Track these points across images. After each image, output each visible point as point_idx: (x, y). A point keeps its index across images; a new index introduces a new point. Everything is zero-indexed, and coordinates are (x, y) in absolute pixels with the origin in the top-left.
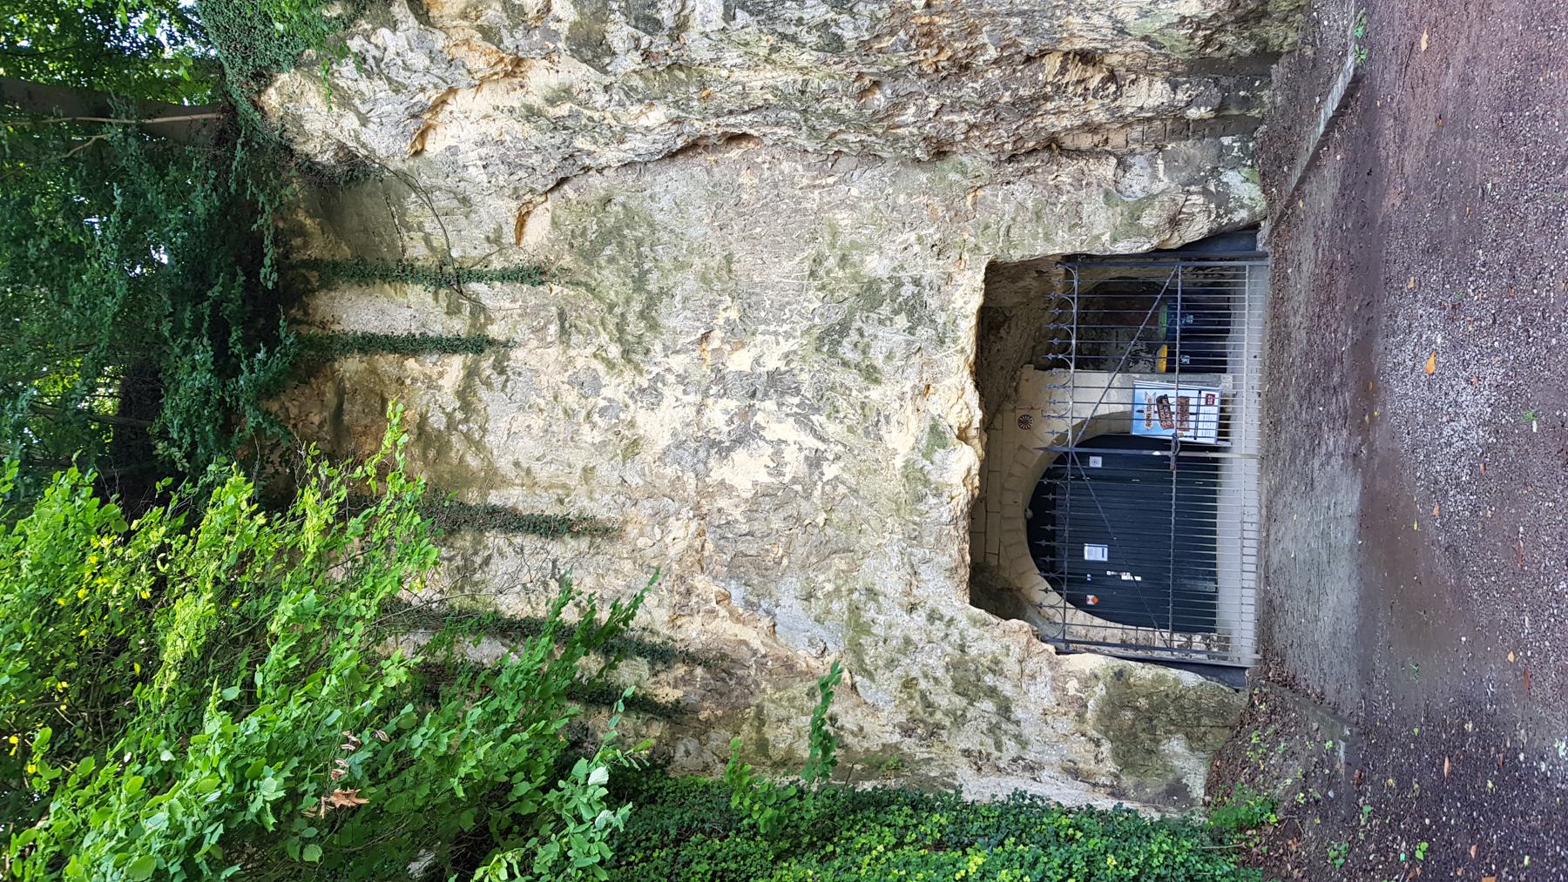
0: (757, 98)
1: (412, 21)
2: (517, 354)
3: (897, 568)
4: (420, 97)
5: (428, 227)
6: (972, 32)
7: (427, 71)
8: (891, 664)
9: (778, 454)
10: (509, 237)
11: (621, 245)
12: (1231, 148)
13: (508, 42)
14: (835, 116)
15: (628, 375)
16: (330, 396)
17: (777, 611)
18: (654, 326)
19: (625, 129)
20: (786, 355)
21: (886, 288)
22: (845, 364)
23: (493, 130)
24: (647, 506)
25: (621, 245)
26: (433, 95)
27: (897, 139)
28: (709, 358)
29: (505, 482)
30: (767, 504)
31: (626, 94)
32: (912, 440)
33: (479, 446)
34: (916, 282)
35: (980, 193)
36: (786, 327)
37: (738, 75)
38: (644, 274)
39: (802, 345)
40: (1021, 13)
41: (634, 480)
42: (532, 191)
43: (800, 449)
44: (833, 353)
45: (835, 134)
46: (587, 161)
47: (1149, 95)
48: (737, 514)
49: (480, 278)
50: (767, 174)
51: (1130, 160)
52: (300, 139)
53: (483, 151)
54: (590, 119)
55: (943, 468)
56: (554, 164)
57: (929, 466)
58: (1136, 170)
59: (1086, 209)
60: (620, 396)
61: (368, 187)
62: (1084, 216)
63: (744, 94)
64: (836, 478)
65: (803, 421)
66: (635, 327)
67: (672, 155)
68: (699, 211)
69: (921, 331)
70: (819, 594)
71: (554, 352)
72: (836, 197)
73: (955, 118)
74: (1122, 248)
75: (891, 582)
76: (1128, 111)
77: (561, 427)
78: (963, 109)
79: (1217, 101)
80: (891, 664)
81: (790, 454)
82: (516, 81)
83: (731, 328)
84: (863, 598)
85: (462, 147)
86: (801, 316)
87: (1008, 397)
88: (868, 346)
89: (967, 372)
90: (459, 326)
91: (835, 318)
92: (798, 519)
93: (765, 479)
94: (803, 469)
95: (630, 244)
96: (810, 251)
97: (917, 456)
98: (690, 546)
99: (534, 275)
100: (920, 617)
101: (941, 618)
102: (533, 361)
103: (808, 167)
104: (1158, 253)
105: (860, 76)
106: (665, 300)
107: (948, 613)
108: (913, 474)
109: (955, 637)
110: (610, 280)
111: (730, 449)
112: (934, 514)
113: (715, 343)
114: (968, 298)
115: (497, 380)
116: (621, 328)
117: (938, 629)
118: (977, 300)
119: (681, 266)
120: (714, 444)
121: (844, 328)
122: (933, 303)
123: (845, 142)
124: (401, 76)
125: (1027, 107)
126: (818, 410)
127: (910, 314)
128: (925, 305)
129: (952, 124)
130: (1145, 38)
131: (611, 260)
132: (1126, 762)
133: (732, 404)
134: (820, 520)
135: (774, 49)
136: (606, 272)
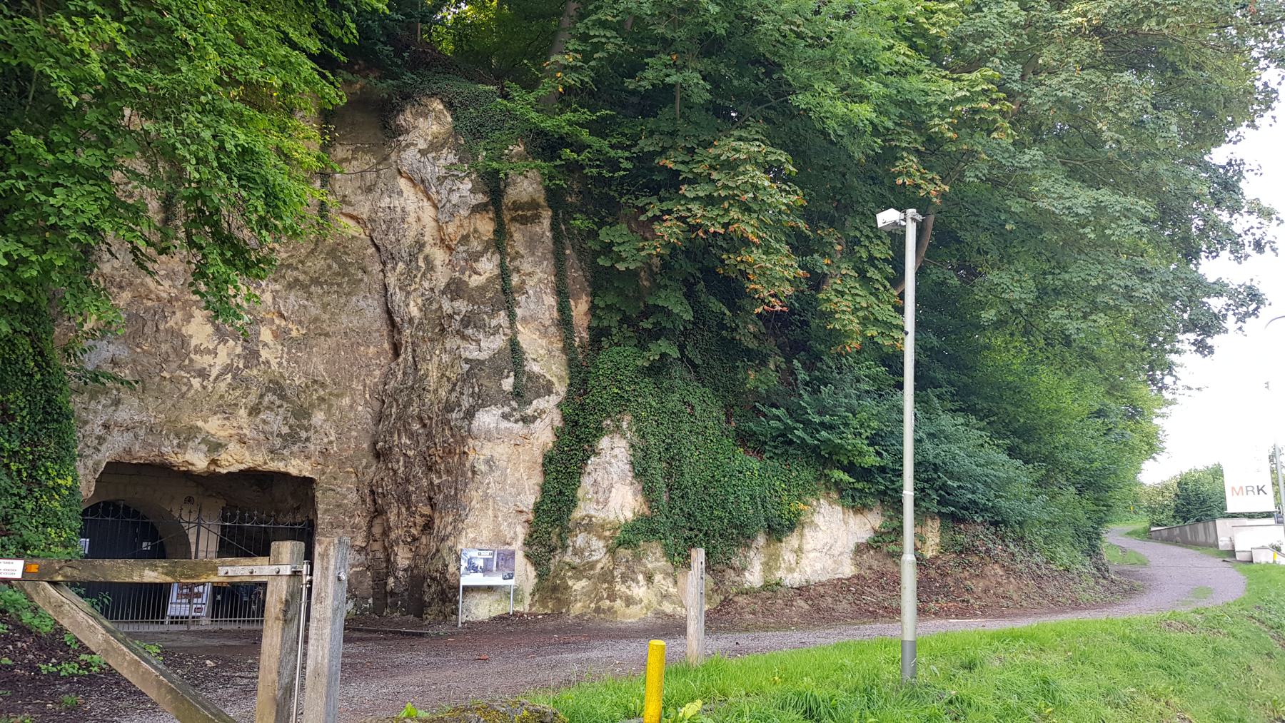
0: (423, 367)
1: (474, 202)
3: (131, 419)
4: (434, 189)
5: (354, 163)
6: (448, 472)
7: (449, 201)
9: (208, 351)
10: (347, 209)
11: (338, 274)
12: (367, 603)
13: (461, 248)
14: (409, 403)
17: (105, 342)
18: (290, 286)
19: (408, 293)
20: (268, 362)
21: (305, 422)
22: (262, 396)
23: (411, 219)
25: (338, 274)
26: (434, 196)
27: (391, 434)
28: (268, 316)
30: (177, 342)
31: (427, 299)
32: (213, 432)
35: (353, 475)
36: (285, 364)
37: (435, 359)
38: (321, 284)
39: (274, 372)
40: (456, 494)
42: (373, 230)
43: (210, 366)
44: (268, 389)
45: (397, 401)
46: (389, 266)
47: (403, 558)
48: (171, 323)
50: (374, 362)
51: (363, 553)
52: (414, 111)
53: (398, 210)
54: (415, 276)
55: (196, 450)
56: (389, 247)
57: (197, 441)
58: (358, 557)
61: (380, 135)
62: (338, 530)
63: (424, 360)
64: (192, 386)
65: (227, 369)
67: (389, 312)
68: (355, 322)
69: (279, 440)
70: (116, 370)
72: (358, 398)
73: (401, 463)
75: (123, 415)
76: (396, 549)
78: (406, 467)
79: (397, 591)
81: (207, 360)
82: (438, 242)
84: (113, 397)
85: (402, 199)
86: (292, 373)
87: (207, 490)
88: (272, 410)
89: (251, 465)
91: (288, 392)
92: (166, 361)
93: (194, 342)
94: (198, 366)
95: (339, 280)
96: (328, 381)
97: (203, 434)
98: (151, 292)
100: (99, 431)
101: (100, 444)
103: (376, 384)
105: (430, 419)
106: (305, 295)
107: (103, 448)
108: (192, 433)
109: (87, 452)
110: (318, 264)
111: (213, 324)
112: (167, 443)
113: (277, 321)
114: (296, 467)
116: (289, 266)
118: (294, 471)
119: (325, 307)
122: (295, 448)
123: (391, 407)
124: (448, 184)
125: (405, 500)
126: (234, 378)
127: (289, 435)
128: (294, 443)
129: (398, 462)
130: (438, 551)
131: (330, 267)
134: (165, 374)
135: (449, 379)
136: (322, 262)
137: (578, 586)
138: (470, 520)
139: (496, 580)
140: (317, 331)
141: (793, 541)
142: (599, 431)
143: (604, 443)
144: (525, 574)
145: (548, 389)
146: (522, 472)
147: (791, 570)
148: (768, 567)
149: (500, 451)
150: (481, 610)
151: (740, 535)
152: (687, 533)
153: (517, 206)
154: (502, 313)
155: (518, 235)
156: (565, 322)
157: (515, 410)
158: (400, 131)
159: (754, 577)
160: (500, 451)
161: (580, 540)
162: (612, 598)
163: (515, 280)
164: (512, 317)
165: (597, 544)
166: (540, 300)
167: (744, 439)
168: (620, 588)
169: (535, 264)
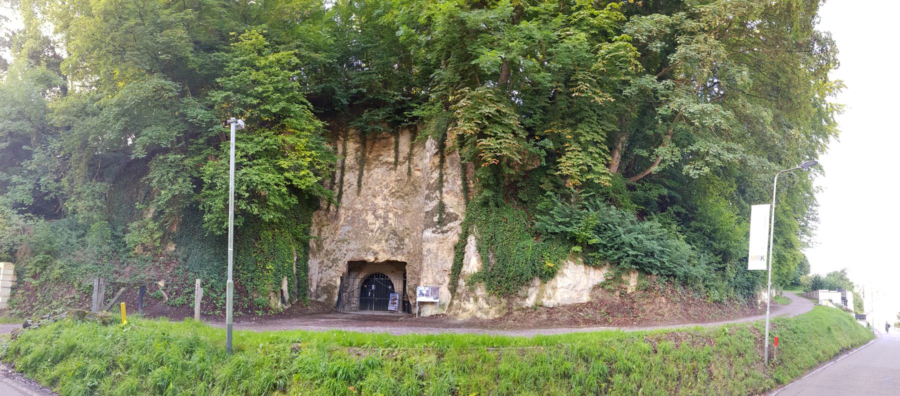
2: (394, 172)
8: (337, 247)
9: (373, 224)
10: (417, 168)
15: (389, 194)
16: (388, 136)
18: (398, 198)
22: (389, 236)
24: (363, 200)
29: (368, 173)
30: (364, 222)
33: (375, 167)
34: (403, 248)
41: (368, 197)
49: (409, 163)
59: (414, 280)
60: (384, 193)
65: (379, 228)
66: (398, 194)
68: (417, 206)
71: (394, 179)
74: (407, 287)
75: (351, 247)
77: (379, 182)
80: (337, 247)
81: (373, 226)
83: (396, 213)
90: (401, 159)
93: (369, 222)
99: (409, 173)
100: (345, 252)
102: (392, 175)
114: (399, 258)
115: (388, 169)
117: (343, 255)
118: (399, 260)
120: (375, 211)
121: (396, 235)
122: (399, 252)
132: (323, 288)
133: (382, 214)
139: (431, 299)
140: (406, 211)
145: (456, 219)
146: (445, 254)
149: (433, 246)
150: (428, 311)
154: (438, 192)
156: (466, 190)
157: (438, 228)
160: (433, 246)
163: (445, 177)
164: (441, 192)
166: (454, 183)
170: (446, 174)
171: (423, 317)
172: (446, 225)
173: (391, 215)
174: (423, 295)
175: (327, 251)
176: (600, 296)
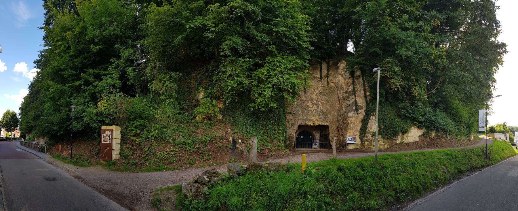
8: (293, 118)
9: (311, 107)
10: (332, 81)
18: (323, 95)
23: (341, 81)
44: (321, 112)
47: (342, 139)
48: (306, 104)
49: (328, 78)
65: (315, 109)
66: (323, 94)
74: (330, 137)
75: (300, 118)
80: (293, 118)
81: (311, 108)
83: (323, 103)
90: (323, 76)
93: (309, 106)
96: (330, 110)
99: (328, 84)
104: (330, 140)
108: (310, 120)
118: (325, 125)
137: (367, 143)
138: (348, 132)
139: (353, 142)
141: (406, 135)
142: (370, 115)
143: (371, 117)
144: (358, 141)
145: (362, 108)
147: (406, 140)
148: (402, 140)
149: (353, 119)
150: (351, 147)
151: (396, 134)
152: (386, 133)
153: (356, 76)
154: (353, 96)
155: (356, 82)
156: (365, 96)
158: (339, 67)
159: (399, 141)
160: (353, 119)
161: (367, 135)
162: (371, 145)
163: (356, 89)
164: (355, 96)
165: (370, 136)
166: (360, 92)
167: (399, 116)
168: (373, 143)
169: (359, 86)
170: (356, 88)
171: (349, 150)
172: (358, 111)
173: (320, 103)
174: (349, 140)
175: (288, 119)
176: (422, 139)
